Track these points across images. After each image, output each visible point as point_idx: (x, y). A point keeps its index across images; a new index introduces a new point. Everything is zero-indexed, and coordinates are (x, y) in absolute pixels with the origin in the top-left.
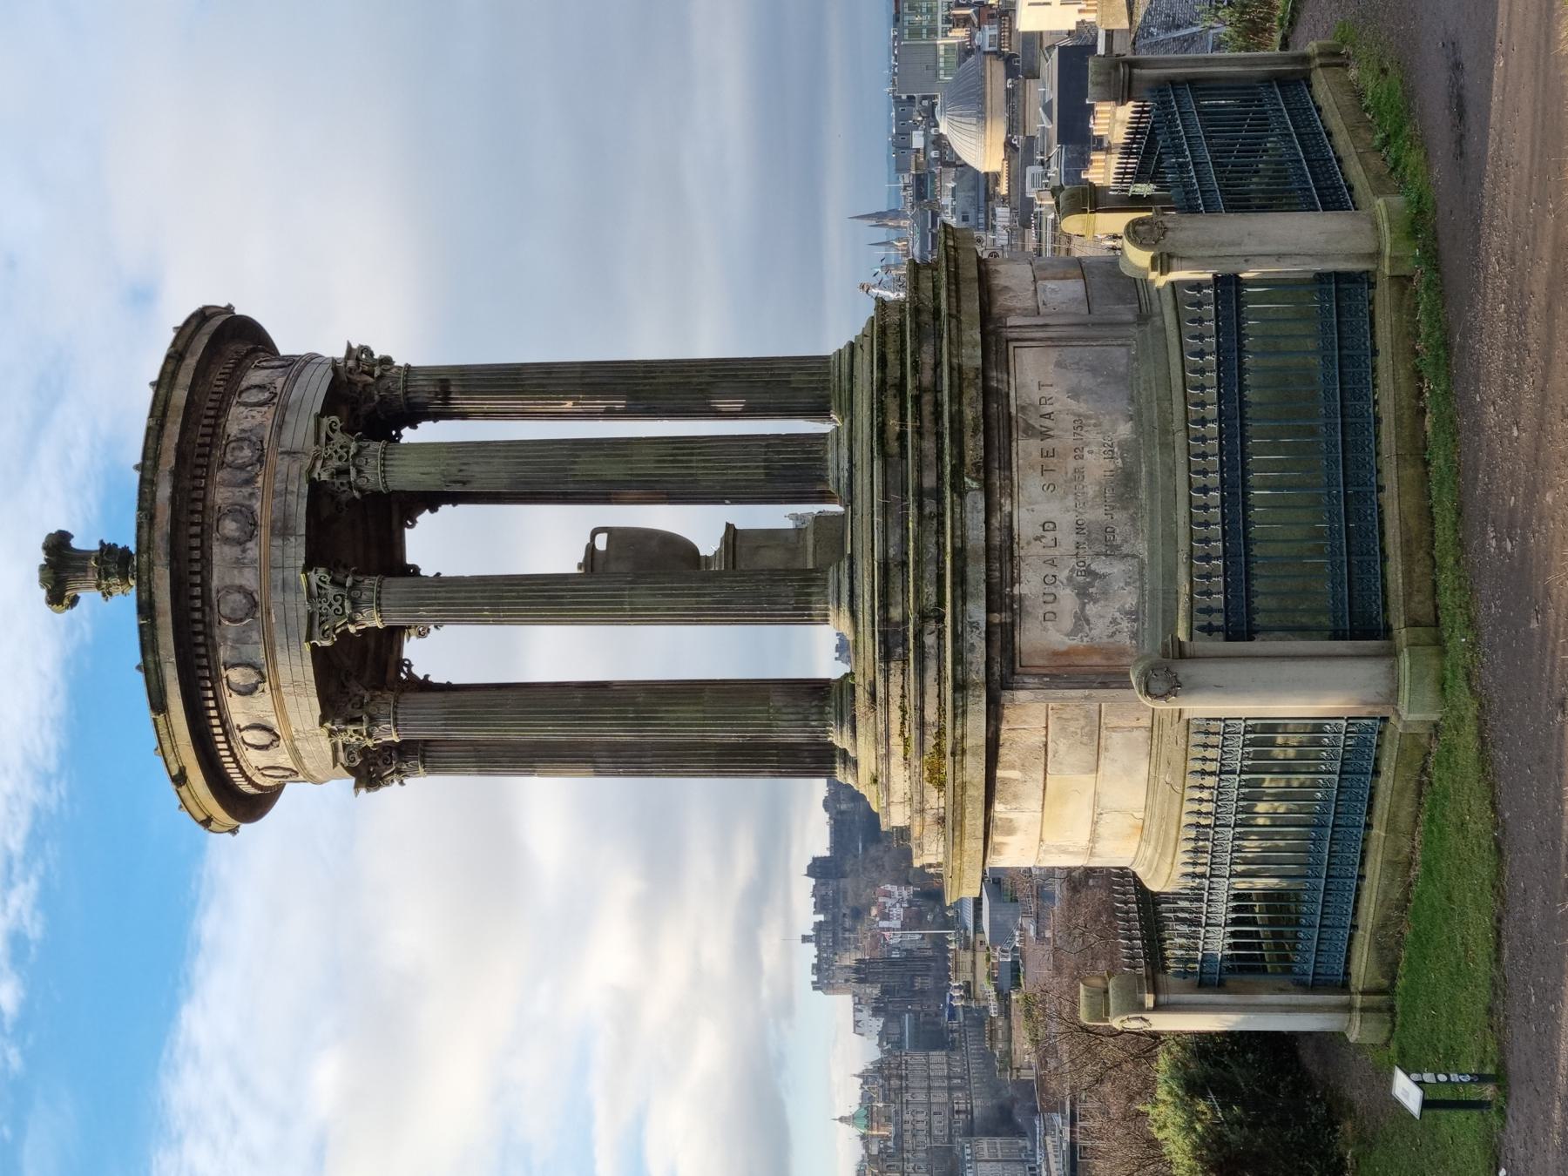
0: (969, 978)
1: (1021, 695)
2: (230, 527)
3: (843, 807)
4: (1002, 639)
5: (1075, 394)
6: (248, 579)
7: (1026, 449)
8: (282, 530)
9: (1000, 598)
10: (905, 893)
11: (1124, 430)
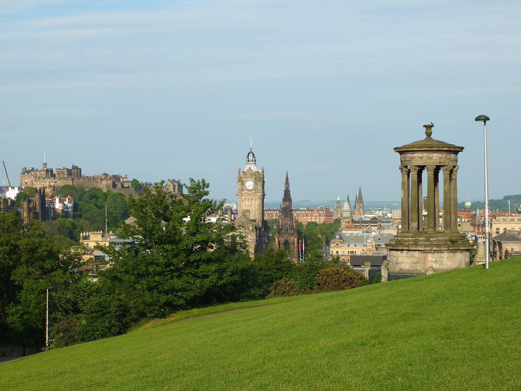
0: (91, 240)
1: (422, 254)
2: (440, 156)
3: (104, 182)
4: (430, 252)
5: (457, 261)
6: (434, 158)
7: (452, 254)
8: (440, 162)
9: (435, 251)
10: (70, 210)
11: (453, 267)
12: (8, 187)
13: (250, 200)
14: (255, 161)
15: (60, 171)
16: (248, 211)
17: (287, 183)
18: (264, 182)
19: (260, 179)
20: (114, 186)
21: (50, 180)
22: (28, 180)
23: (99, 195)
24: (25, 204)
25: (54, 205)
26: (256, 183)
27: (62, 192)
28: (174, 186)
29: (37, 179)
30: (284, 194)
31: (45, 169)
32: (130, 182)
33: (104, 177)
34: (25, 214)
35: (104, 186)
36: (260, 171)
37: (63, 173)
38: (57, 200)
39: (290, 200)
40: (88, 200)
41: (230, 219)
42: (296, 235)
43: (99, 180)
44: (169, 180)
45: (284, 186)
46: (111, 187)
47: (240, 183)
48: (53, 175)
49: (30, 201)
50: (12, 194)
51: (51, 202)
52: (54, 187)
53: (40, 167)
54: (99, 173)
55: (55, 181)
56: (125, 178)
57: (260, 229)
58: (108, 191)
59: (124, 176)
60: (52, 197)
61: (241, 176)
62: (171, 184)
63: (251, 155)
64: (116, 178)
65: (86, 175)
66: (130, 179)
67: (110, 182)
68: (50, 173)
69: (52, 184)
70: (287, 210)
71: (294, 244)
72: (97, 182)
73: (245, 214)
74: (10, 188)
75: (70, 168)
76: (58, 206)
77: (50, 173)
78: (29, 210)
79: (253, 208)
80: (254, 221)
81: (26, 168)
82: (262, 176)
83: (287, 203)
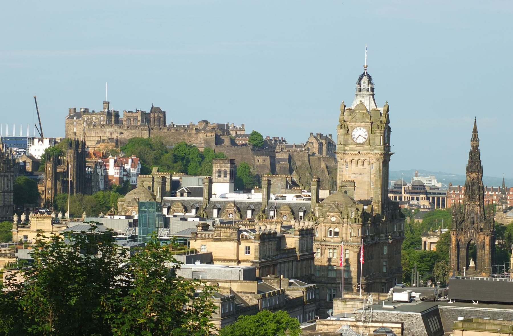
3: (201, 135)
12: (33, 138)
13: (360, 163)
14: (372, 90)
15: (130, 114)
16: (353, 184)
17: (475, 139)
18: (388, 130)
19: (383, 126)
20: (218, 141)
21: (112, 130)
22: (77, 130)
23: (190, 156)
24: (49, 167)
25: (106, 169)
26: (371, 132)
27: (122, 148)
28: (321, 144)
29: (92, 127)
30: (468, 158)
31: (106, 110)
32: (247, 135)
33: (201, 127)
34: (49, 184)
35: (200, 141)
36: (382, 110)
37: (135, 119)
38: (112, 161)
39: (480, 170)
40: (170, 163)
41: (314, 198)
42: (488, 231)
43: (194, 131)
44: (312, 134)
45: (470, 143)
46: (213, 144)
47: (342, 131)
48: (118, 122)
49: (58, 162)
50: (38, 150)
51: (101, 165)
52: (117, 141)
53: (99, 108)
54: (195, 121)
55: (120, 130)
56: (240, 129)
57: (376, 219)
58: (207, 150)
59: (238, 126)
60: (105, 156)
61: (346, 117)
62: (315, 141)
63: (365, 79)
64: (224, 129)
65: (176, 123)
66: (248, 131)
67: (211, 136)
68: (113, 118)
69: (115, 136)
70: (474, 188)
71: (484, 247)
72: (190, 135)
73: (344, 189)
74: (36, 141)
75: (148, 111)
76: (113, 171)
77: (113, 118)
78: (56, 176)
79: (366, 179)
80: (367, 203)
81: (75, 109)
82: (383, 119)
83: (474, 175)
